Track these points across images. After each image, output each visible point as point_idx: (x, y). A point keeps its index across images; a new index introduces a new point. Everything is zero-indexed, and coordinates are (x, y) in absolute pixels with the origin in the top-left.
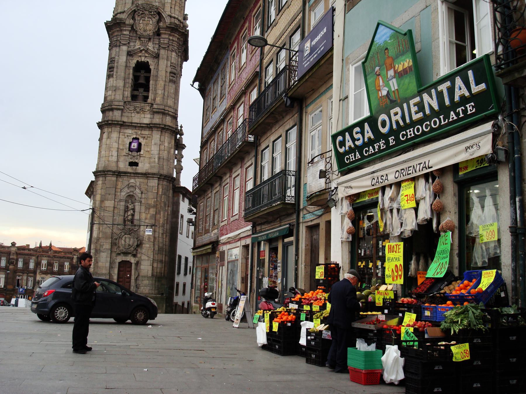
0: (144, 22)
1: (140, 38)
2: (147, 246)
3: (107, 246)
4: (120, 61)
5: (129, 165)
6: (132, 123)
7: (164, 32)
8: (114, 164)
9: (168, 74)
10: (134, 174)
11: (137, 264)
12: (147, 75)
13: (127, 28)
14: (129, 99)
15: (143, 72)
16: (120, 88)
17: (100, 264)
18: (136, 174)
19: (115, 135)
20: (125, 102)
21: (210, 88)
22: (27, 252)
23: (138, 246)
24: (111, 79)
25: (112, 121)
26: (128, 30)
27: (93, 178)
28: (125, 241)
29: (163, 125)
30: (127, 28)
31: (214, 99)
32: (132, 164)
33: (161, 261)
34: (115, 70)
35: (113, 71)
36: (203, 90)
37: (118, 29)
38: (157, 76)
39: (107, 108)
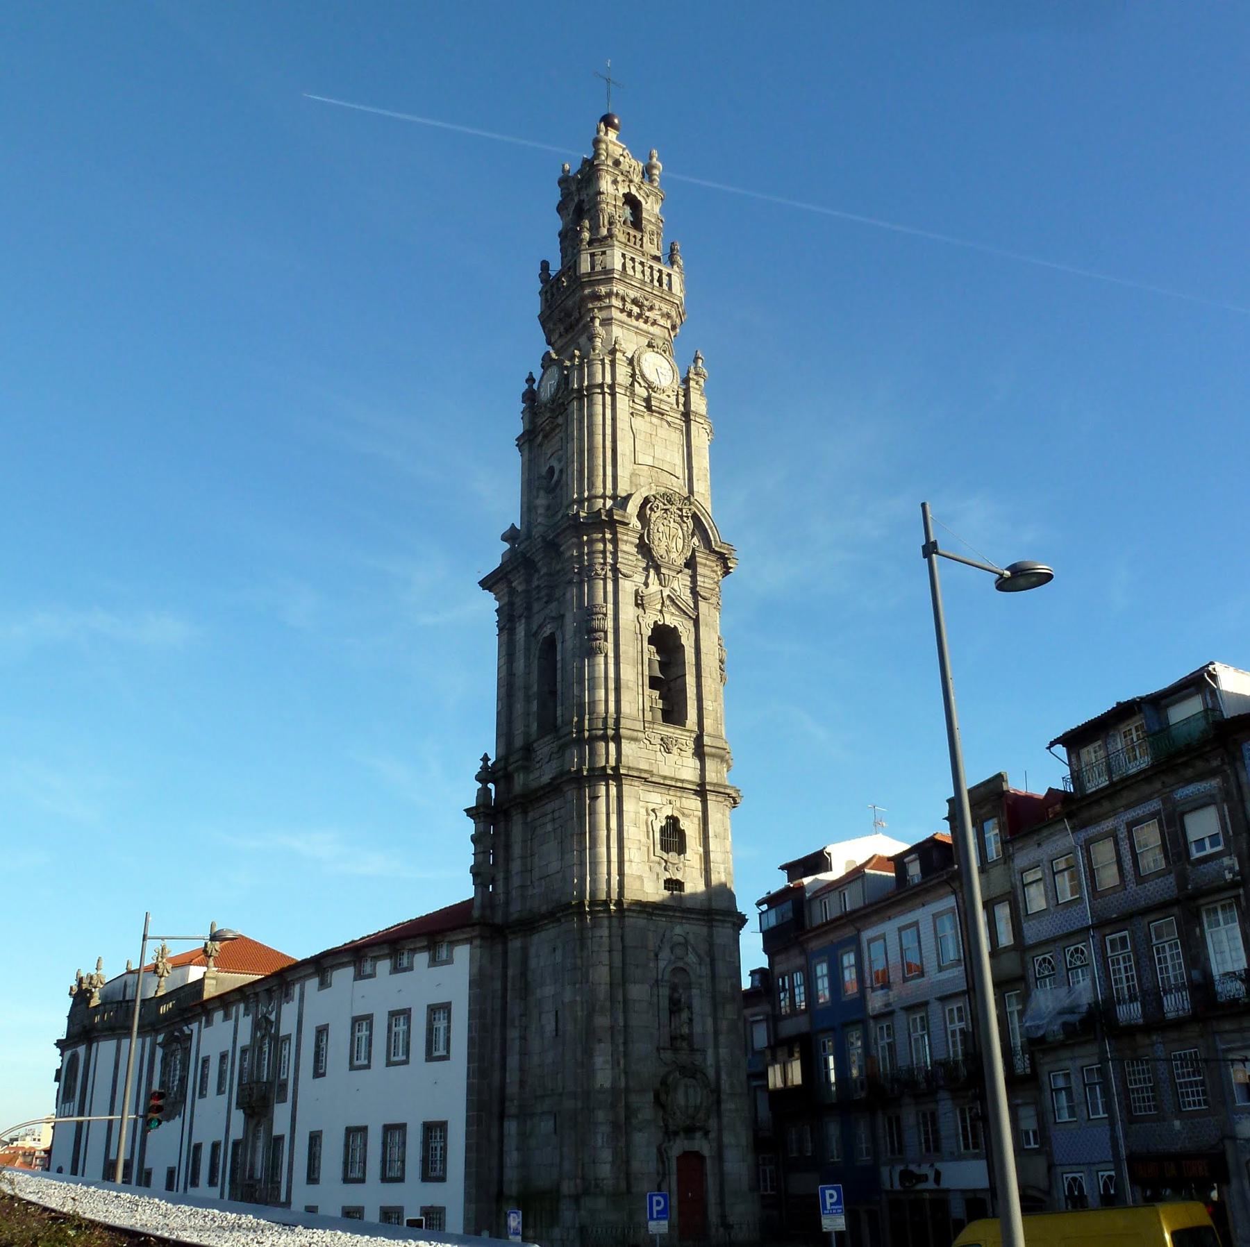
1: (657, 569)
2: (728, 1106)
6: (665, 778)
7: (704, 561)
8: (637, 885)
9: (717, 664)
11: (720, 1157)
14: (648, 716)
16: (631, 684)
17: (636, 1165)
25: (629, 768)
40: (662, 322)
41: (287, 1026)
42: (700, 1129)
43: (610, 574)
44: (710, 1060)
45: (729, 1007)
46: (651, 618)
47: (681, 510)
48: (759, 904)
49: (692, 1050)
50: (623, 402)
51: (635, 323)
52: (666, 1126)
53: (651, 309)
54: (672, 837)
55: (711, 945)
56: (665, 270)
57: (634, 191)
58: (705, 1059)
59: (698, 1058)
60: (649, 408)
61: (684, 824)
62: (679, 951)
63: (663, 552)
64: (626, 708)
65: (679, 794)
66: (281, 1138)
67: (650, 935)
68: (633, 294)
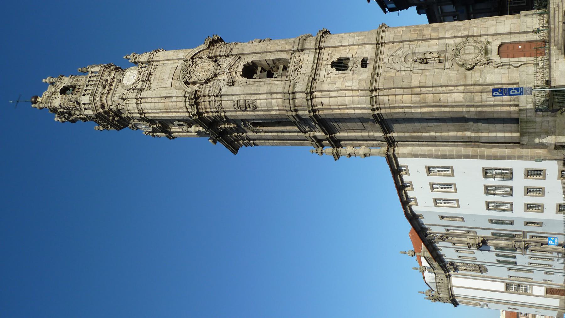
0: (199, 71)
1: (216, 75)
2: (475, 31)
6: (312, 69)
8: (362, 82)
12: (259, 69)
14: (284, 78)
15: (255, 76)
16: (269, 88)
19: (325, 87)
24: (258, 102)
25: (307, 88)
26: (205, 89)
28: (469, 54)
32: (364, 63)
34: (248, 98)
41: (442, 230)
42: (486, 45)
43: (218, 99)
44: (451, 41)
45: (425, 32)
47: (190, 65)
48: (385, 12)
49: (446, 51)
51: (113, 88)
52: (484, 64)
53: (107, 81)
54: (340, 65)
55: (394, 42)
56: (90, 74)
57: (59, 90)
58: (451, 44)
59: (450, 48)
61: (335, 59)
62: (397, 59)
63: (209, 73)
64: (280, 89)
65: (321, 61)
66: (494, 234)
67: (388, 75)
68: (100, 89)
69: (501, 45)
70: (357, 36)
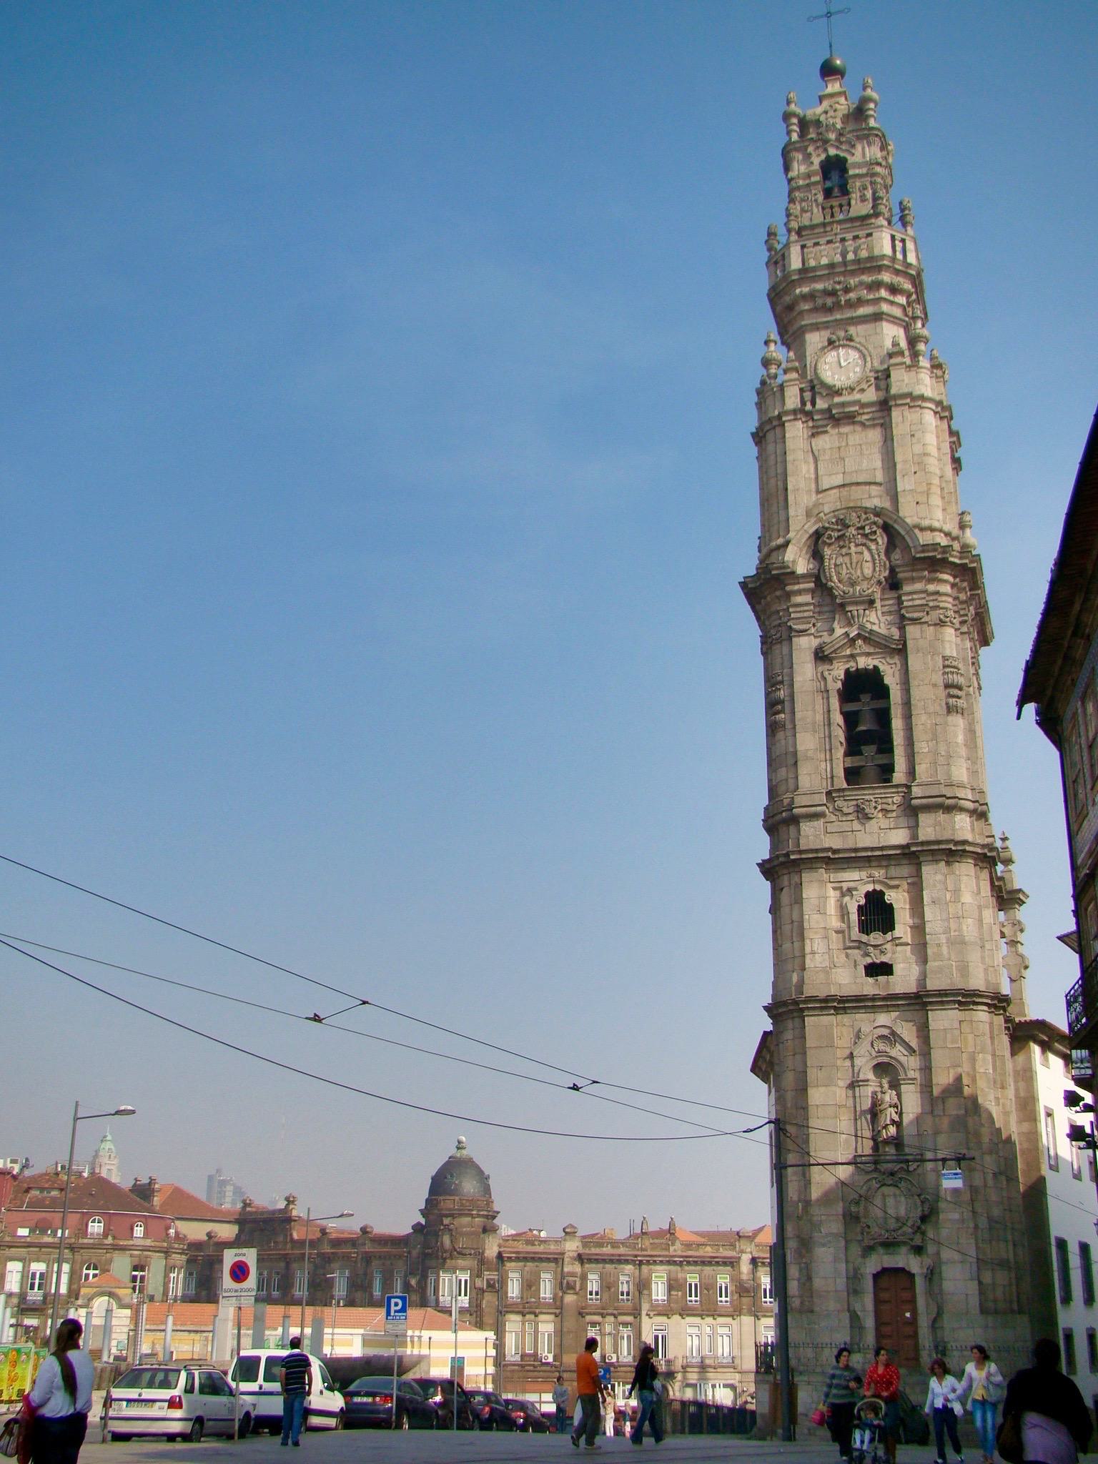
0: (847, 559)
2: (950, 1216)
3: (835, 1227)
4: (798, 679)
5: (867, 975)
6: (856, 850)
7: (906, 575)
8: (822, 976)
9: (942, 693)
10: (884, 999)
11: (932, 1274)
12: (879, 704)
13: (802, 586)
15: (865, 698)
16: (810, 754)
17: (818, 1283)
18: (890, 1001)
20: (829, 793)
21: (1075, 714)
22: (607, 1250)
23: (924, 1219)
24: (780, 735)
25: (801, 852)
27: (768, 1025)
29: (948, 842)
30: (802, 586)
31: (1090, 747)
32: (879, 970)
33: (1003, 1264)
35: (778, 712)
36: (1051, 724)
37: (778, 593)
38: (907, 704)
39: (778, 818)
40: (871, 297)
46: (838, 671)
50: (796, 432)
53: (847, 290)
54: (876, 914)
57: (832, 152)
60: (832, 417)
61: (891, 897)
62: (881, 1046)
65: (884, 863)
68: (819, 286)
69: (911, 1276)
70: (948, 939)
